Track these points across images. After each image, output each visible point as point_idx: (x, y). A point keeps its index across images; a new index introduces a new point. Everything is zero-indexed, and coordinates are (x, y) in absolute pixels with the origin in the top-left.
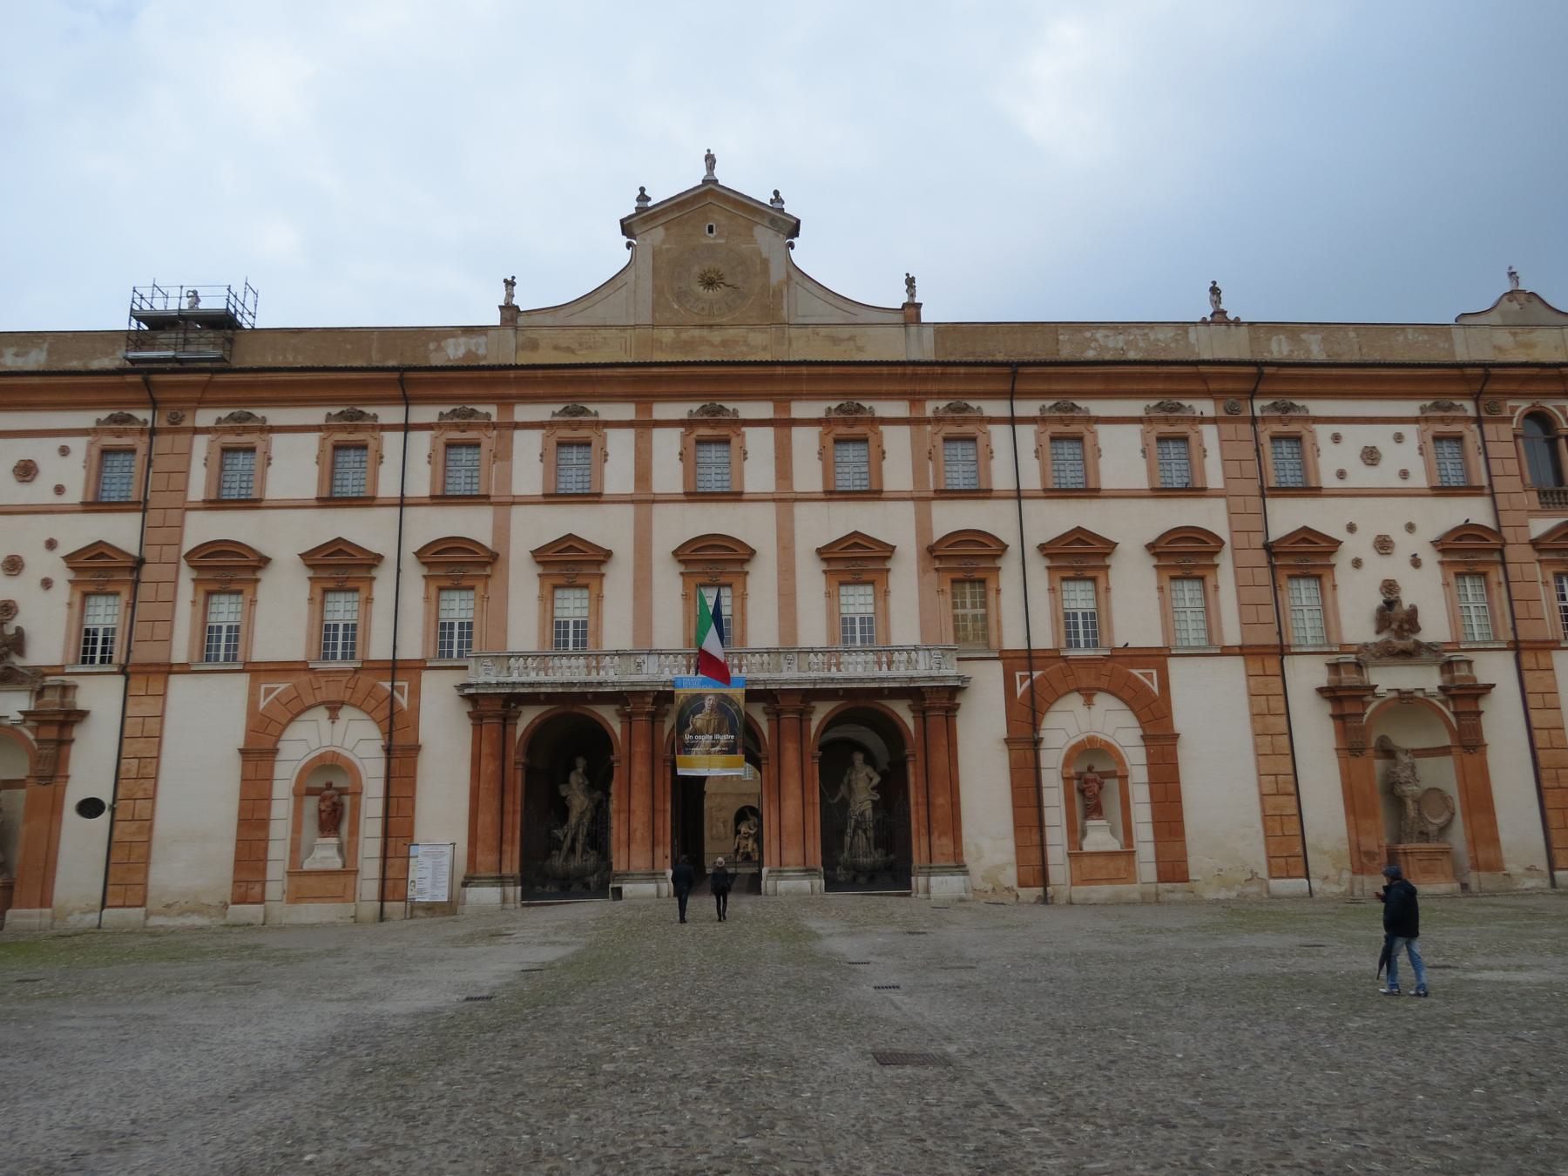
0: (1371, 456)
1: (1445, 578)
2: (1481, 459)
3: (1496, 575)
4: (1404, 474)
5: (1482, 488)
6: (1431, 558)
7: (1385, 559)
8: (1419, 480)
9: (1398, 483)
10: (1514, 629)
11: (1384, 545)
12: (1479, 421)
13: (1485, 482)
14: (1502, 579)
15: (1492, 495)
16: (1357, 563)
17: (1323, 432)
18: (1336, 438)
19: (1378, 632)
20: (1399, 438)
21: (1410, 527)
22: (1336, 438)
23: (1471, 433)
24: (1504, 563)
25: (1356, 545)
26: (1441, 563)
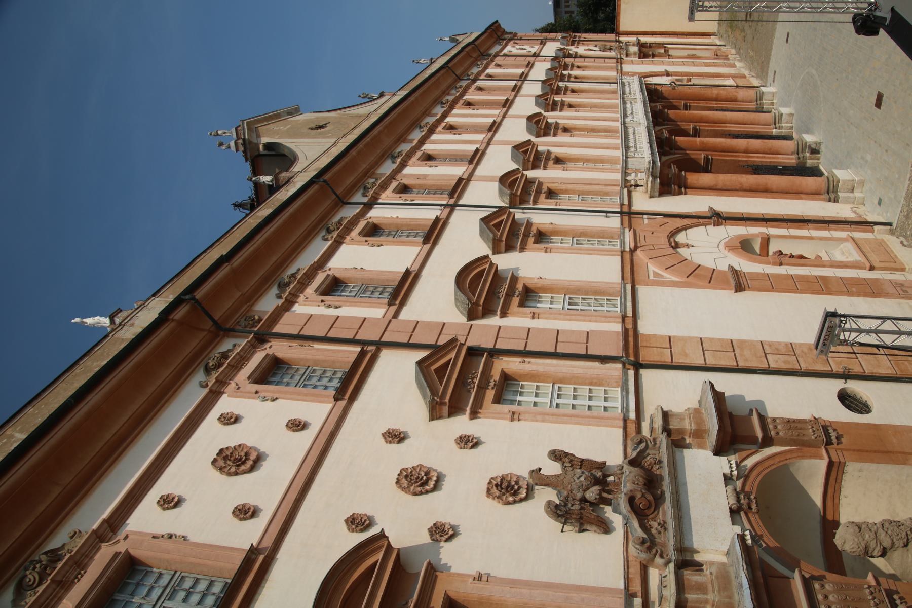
0: (237, 461)
1: (498, 416)
2: (317, 346)
3: (512, 364)
4: (297, 426)
5: (362, 354)
6: (462, 424)
7: (446, 485)
8: (317, 411)
9: (305, 439)
10: (604, 359)
11: (420, 481)
12: (261, 339)
13: (358, 349)
14: (520, 359)
15: (380, 345)
16: (442, 533)
17: (146, 519)
18: (170, 502)
19: (605, 527)
20: (230, 420)
21: (396, 437)
22: (170, 502)
23: (278, 348)
24: (494, 353)
25: (404, 524)
26: (474, 415)
